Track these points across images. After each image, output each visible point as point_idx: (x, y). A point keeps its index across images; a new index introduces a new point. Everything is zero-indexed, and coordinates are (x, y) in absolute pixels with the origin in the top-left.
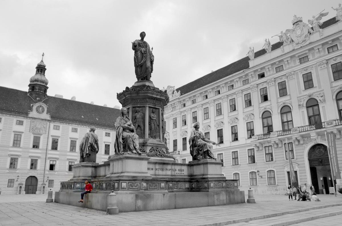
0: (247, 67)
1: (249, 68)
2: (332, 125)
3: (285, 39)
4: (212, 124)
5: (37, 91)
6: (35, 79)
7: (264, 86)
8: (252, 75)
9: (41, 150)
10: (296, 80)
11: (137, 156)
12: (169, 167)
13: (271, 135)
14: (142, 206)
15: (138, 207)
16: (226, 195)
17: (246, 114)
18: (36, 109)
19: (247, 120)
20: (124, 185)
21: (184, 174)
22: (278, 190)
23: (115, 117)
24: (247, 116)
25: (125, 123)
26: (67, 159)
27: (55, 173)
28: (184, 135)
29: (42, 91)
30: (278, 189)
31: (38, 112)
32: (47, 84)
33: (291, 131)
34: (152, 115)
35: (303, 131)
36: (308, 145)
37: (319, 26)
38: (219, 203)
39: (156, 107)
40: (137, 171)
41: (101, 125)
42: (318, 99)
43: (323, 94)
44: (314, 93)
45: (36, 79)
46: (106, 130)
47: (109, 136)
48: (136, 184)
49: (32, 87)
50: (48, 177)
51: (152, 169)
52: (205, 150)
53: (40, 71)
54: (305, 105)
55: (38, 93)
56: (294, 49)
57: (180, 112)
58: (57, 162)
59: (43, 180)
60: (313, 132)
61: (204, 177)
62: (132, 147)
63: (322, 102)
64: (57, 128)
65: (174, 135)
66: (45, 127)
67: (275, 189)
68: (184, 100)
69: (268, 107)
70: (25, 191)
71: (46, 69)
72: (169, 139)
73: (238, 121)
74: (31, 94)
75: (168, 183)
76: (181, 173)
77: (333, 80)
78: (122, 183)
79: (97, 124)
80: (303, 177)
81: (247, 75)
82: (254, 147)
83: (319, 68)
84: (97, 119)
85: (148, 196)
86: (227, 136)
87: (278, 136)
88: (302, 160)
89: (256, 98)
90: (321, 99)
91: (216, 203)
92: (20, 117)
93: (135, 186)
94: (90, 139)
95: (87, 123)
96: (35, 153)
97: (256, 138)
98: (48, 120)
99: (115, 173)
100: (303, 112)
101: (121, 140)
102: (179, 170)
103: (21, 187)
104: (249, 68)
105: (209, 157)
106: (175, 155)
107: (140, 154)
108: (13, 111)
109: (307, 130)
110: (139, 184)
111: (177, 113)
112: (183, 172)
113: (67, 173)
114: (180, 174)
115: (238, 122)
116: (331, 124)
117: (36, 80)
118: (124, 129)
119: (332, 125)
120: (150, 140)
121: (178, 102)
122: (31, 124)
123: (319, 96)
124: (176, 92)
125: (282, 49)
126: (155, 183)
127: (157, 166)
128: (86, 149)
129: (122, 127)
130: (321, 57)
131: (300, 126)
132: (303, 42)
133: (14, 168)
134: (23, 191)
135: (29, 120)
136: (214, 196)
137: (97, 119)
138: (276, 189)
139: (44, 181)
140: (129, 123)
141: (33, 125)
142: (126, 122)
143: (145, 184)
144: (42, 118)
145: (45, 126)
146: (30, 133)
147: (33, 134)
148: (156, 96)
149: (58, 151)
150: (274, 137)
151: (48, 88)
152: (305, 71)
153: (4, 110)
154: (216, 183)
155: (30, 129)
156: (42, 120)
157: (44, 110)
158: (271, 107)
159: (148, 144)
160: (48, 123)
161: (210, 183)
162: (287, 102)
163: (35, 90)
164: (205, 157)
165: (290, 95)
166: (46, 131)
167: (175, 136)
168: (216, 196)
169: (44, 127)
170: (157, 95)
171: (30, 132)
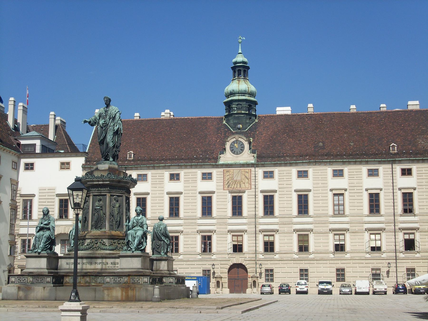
5: (236, 112)
12: (99, 261)
14: (23, 296)
15: (20, 297)
16: (122, 291)
18: (231, 148)
21: (118, 267)
23: (395, 131)
26: (293, 231)
27: (275, 257)
31: (234, 153)
38: (109, 299)
39: (102, 194)
40: (36, 267)
45: (231, 92)
47: (377, 175)
48: (23, 279)
49: (228, 105)
50: (261, 264)
55: (238, 117)
58: (277, 236)
62: (37, 245)
64: (269, 175)
70: (228, 288)
71: (248, 68)
75: (85, 277)
76: (114, 267)
84: (352, 144)
85: (29, 288)
91: (106, 298)
93: (23, 281)
98: (252, 165)
102: (111, 263)
108: (197, 159)
110: (26, 279)
112: (117, 266)
113: (296, 256)
114: (113, 268)
117: (232, 94)
120: (92, 232)
126: (41, 278)
135: (221, 170)
136: (103, 291)
137: (352, 144)
140: (46, 222)
141: (228, 177)
143: (31, 279)
144: (242, 162)
145: (247, 175)
146: (225, 191)
147: (230, 192)
148: (97, 183)
149: (276, 217)
153: (182, 159)
154: (115, 278)
157: (244, 147)
159: (87, 237)
160: (253, 169)
161: (106, 278)
166: (251, 184)
168: (106, 292)
170: (98, 181)
171: (224, 190)
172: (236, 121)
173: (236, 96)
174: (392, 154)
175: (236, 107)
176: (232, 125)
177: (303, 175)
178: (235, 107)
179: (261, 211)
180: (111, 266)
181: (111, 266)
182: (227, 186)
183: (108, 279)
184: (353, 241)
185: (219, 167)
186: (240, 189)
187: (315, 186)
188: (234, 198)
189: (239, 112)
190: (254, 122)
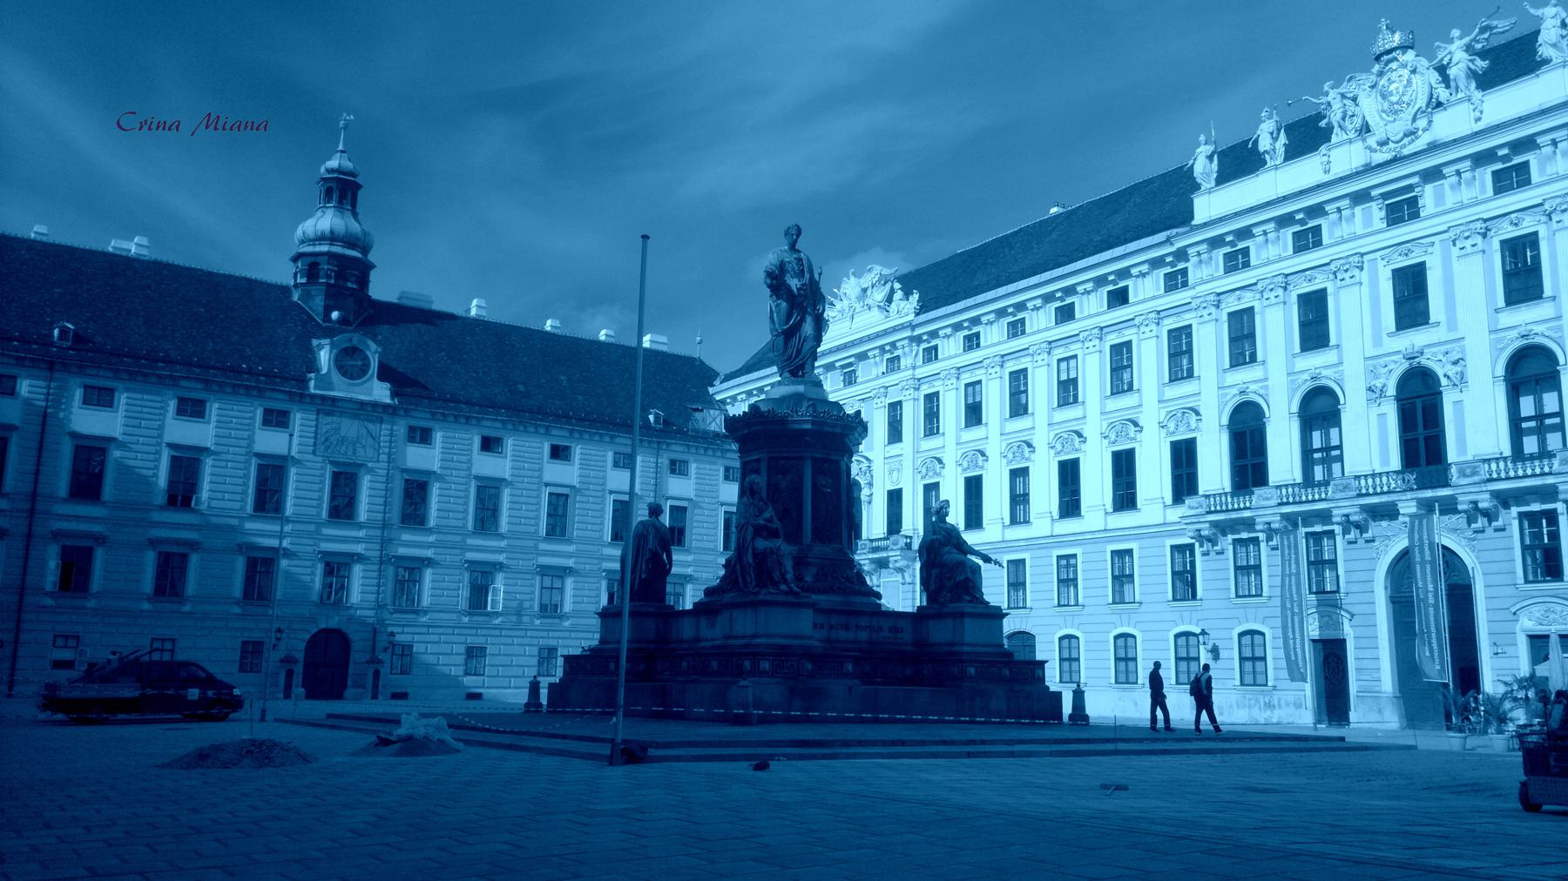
0: (1182, 217)
1: (1193, 223)
2: (1476, 479)
3: (1339, 116)
4: (1041, 439)
5: (333, 281)
6: (319, 234)
8: (1199, 254)
9: (360, 526)
10: (1365, 289)
11: (790, 599)
12: (864, 621)
13: (1254, 498)
17: (1174, 406)
19: (1174, 433)
20: (765, 665)
22: (1274, 706)
24: (1171, 415)
25: (758, 514)
28: (931, 474)
29: (351, 282)
30: (1276, 703)
32: (365, 250)
33: (1330, 489)
34: (822, 480)
35: (1371, 491)
36: (1391, 543)
41: (594, 420)
42: (1440, 373)
43: (1460, 356)
44: (1429, 346)
46: (618, 440)
51: (822, 627)
52: (958, 579)
53: (335, 197)
54: (1391, 390)
56: (1368, 161)
57: (916, 382)
59: (370, 643)
60: (1409, 497)
61: (955, 649)
62: (776, 576)
63: (1455, 385)
65: (891, 473)
66: (374, 434)
67: (1265, 702)
68: (934, 334)
69: (1253, 387)
71: (358, 186)
72: (870, 484)
73: (1141, 431)
74: (306, 296)
77: (1501, 302)
78: (761, 662)
79: (580, 419)
80: (1365, 664)
81: (1182, 255)
82: (1192, 538)
83: (1455, 251)
84: (580, 398)
86: (1097, 484)
87: (1280, 504)
88: (1365, 598)
89: (1210, 344)
90: (1452, 371)
92: (276, 395)
94: (651, 538)
95: (540, 417)
96: (339, 539)
97: (1201, 506)
98: (385, 407)
99: (736, 638)
100: (1382, 416)
101: (750, 558)
103: (290, 673)
105: (968, 598)
106: (892, 550)
107: (796, 594)
109: (1385, 489)
111: (904, 383)
112: (900, 635)
115: (1138, 435)
116: (1474, 473)
118: (760, 531)
119: (1476, 479)
121: (912, 339)
122: (317, 426)
123: (1444, 360)
124: (899, 295)
125: (1325, 158)
127: (835, 620)
128: (639, 567)
129: (752, 525)
130: (1463, 207)
131: (1367, 470)
132: (1406, 135)
133: (261, 597)
134: (297, 686)
138: (1270, 702)
139: (374, 648)
140: (767, 515)
141: (328, 427)
142: (761, 512)
146: (316, 459)
147: (332, 463)
150: (1264, 506)
151: (372, 267)
152: (1400, 258)
155: (315, 445)
156: (362, 404)
158: (1266, 387)
162: (1325, 373)
163: (321, 281)
164: (958, 599)
165: (1338, 346)
167: (895, 474)
169: (372, 435)
171: (314, 453)
172: (332, 303)
173: (334, 245)
174: (657, 431)
175: (335, 271)
176: (321, 309)
177: (489, 445)
178: (332, 271)
179: (395, 515)
180: (888, 635)
181: (888, 635)
182: (323, 447)
183: (972, 670)
184: (579, 592)
185: (308, 400)
186: (354, 458)
187: (516, 472)
188: (336, 476)
189: (341, 283)
190: (366, 313)
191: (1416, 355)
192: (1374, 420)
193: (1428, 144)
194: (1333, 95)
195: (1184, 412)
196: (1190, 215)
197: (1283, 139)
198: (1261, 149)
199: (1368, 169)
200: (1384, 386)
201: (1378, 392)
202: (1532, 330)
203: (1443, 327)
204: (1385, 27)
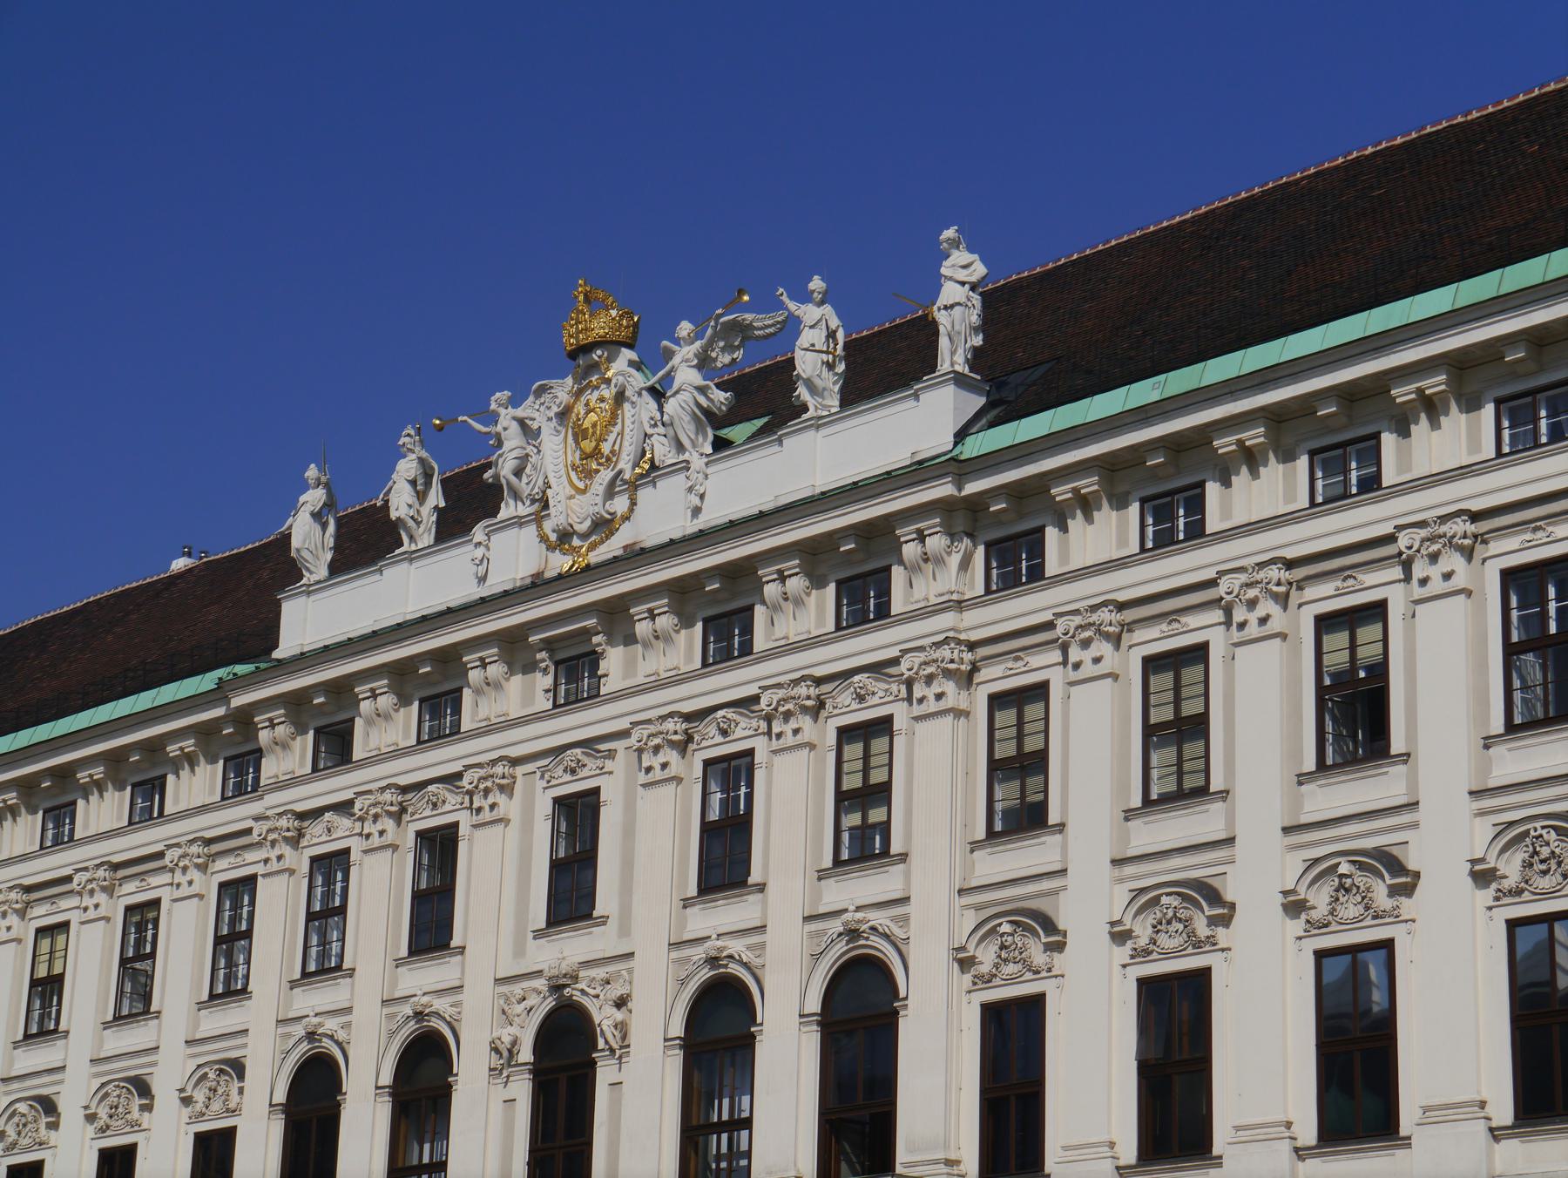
1: (276, 654)
7: (447, 807)
10: (513, 831)
37: (707, 413)
54: (526, 1055)
81: (244, 719)
104: (280, 662)
125: (479, 552)
191: (564, 981)
192: (497, 1108)
193: (625, 547)
194: (506, 417)
195: (221, 1071)
196: (269, 634)
197: (436, 498)
198: (393, 515)
199: (538, 586)
200: (514, 1043)
201: (505, 1054)
202: (720, 950)
203: (612, 924)
204: (581, 298)
